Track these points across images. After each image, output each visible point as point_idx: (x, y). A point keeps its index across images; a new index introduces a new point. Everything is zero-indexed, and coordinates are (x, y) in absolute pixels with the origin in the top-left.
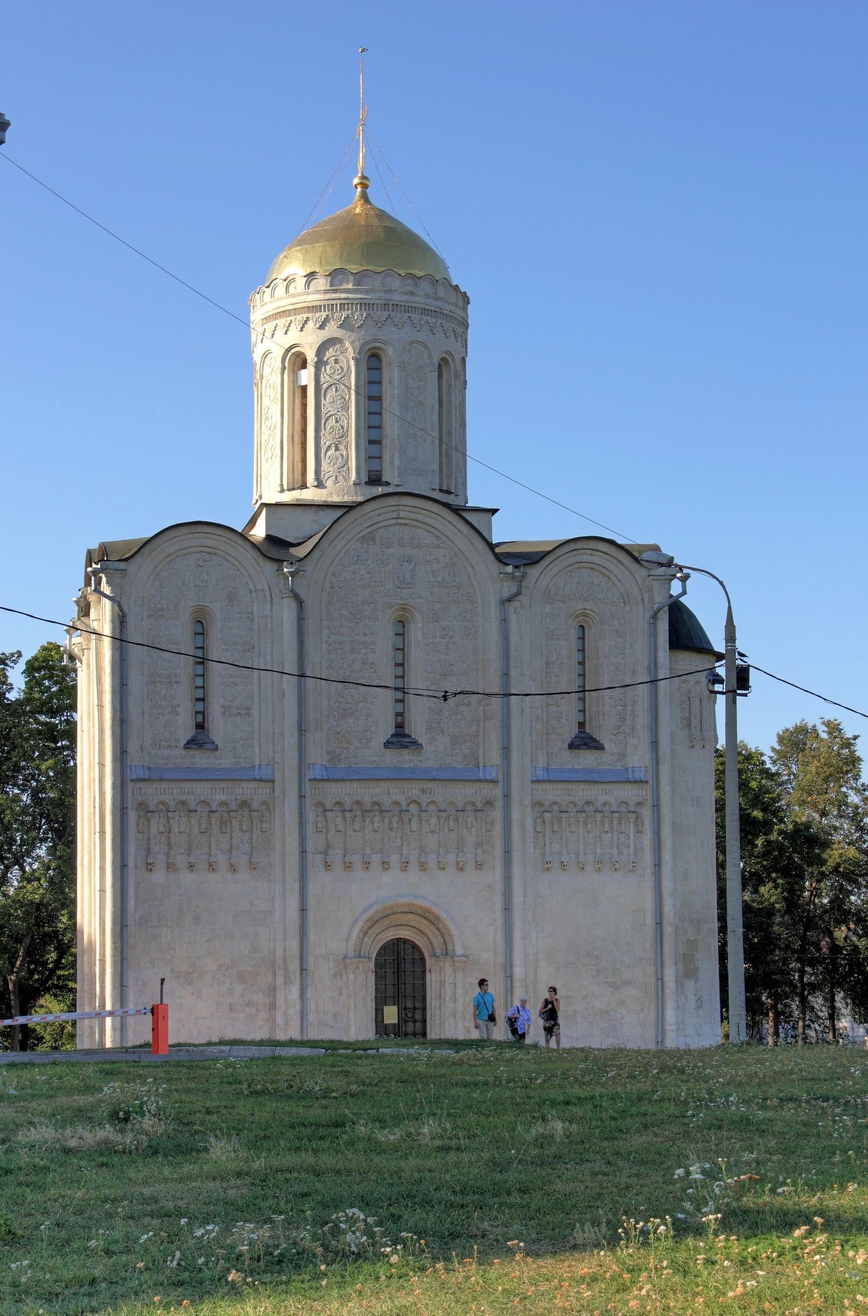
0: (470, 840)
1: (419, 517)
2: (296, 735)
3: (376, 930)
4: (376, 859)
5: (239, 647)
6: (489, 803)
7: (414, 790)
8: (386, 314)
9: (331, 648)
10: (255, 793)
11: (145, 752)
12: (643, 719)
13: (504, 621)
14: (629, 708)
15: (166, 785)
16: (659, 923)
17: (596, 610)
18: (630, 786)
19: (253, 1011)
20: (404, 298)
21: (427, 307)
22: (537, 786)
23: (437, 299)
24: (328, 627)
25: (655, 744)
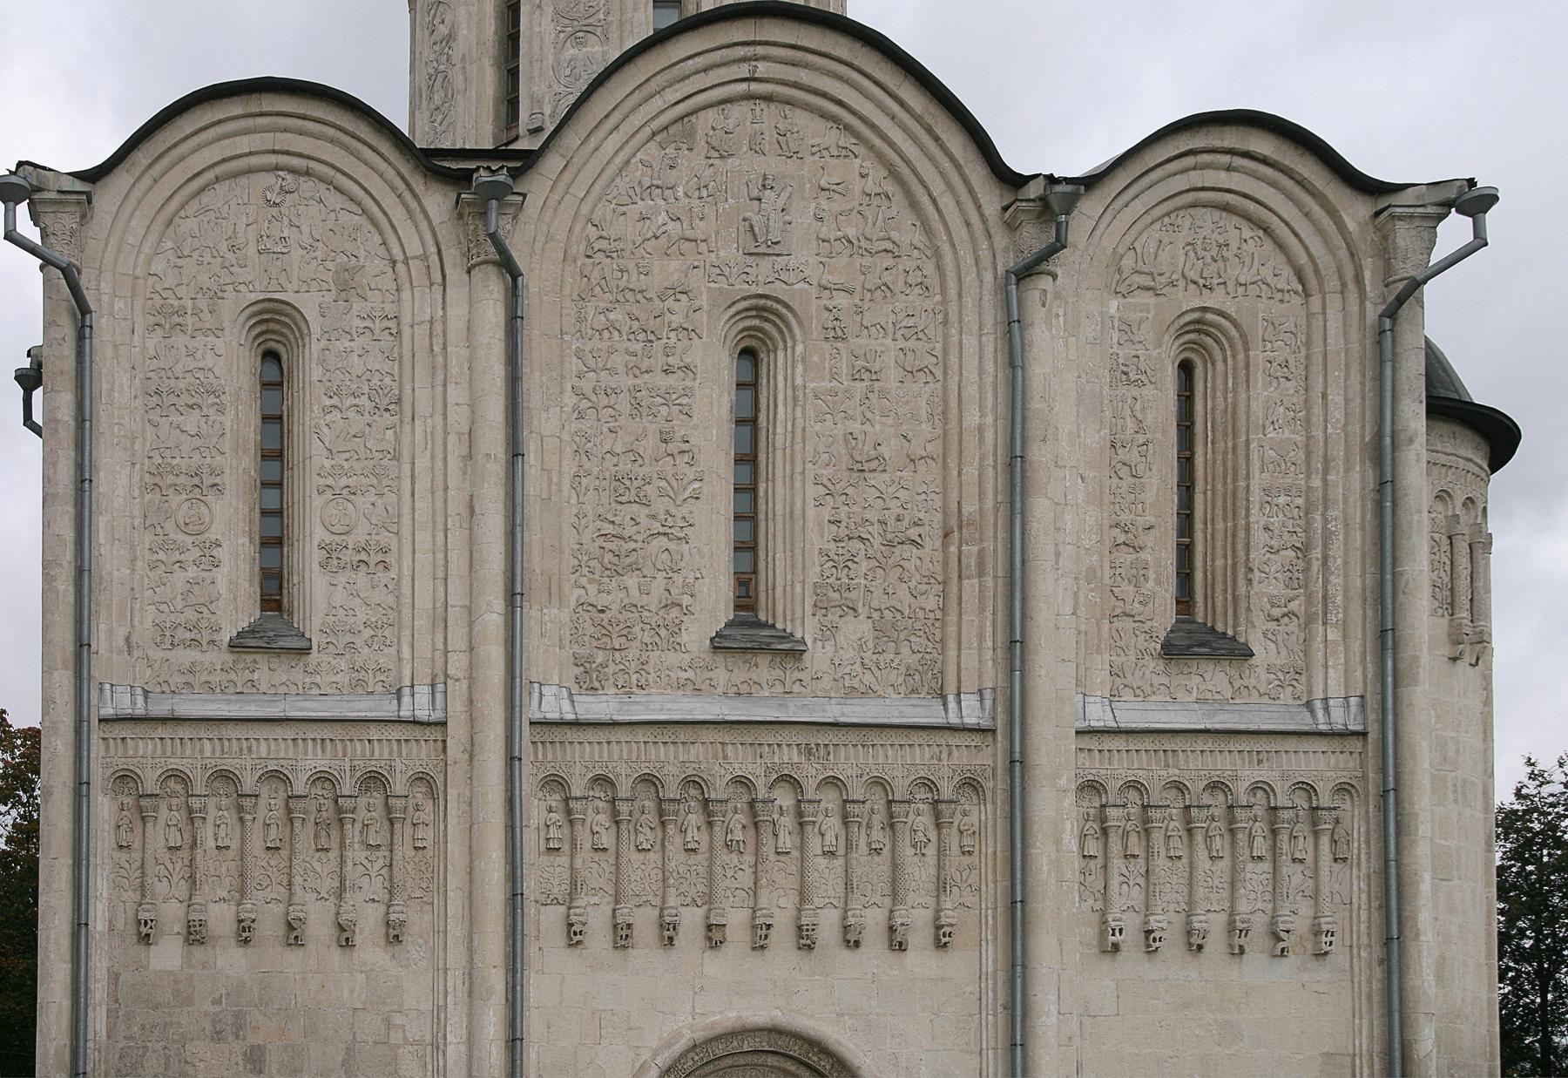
0: (919, 872)
1: (804, 76)
4: (691, 919)
5: (364, 400)
9: (585, 404)
11: (136, 653)
12: (1348, 576)
15: (185, 732)
17: (1232, 311)
18: (1319, 745)
22: (1087, 742)
24: (579, 354)
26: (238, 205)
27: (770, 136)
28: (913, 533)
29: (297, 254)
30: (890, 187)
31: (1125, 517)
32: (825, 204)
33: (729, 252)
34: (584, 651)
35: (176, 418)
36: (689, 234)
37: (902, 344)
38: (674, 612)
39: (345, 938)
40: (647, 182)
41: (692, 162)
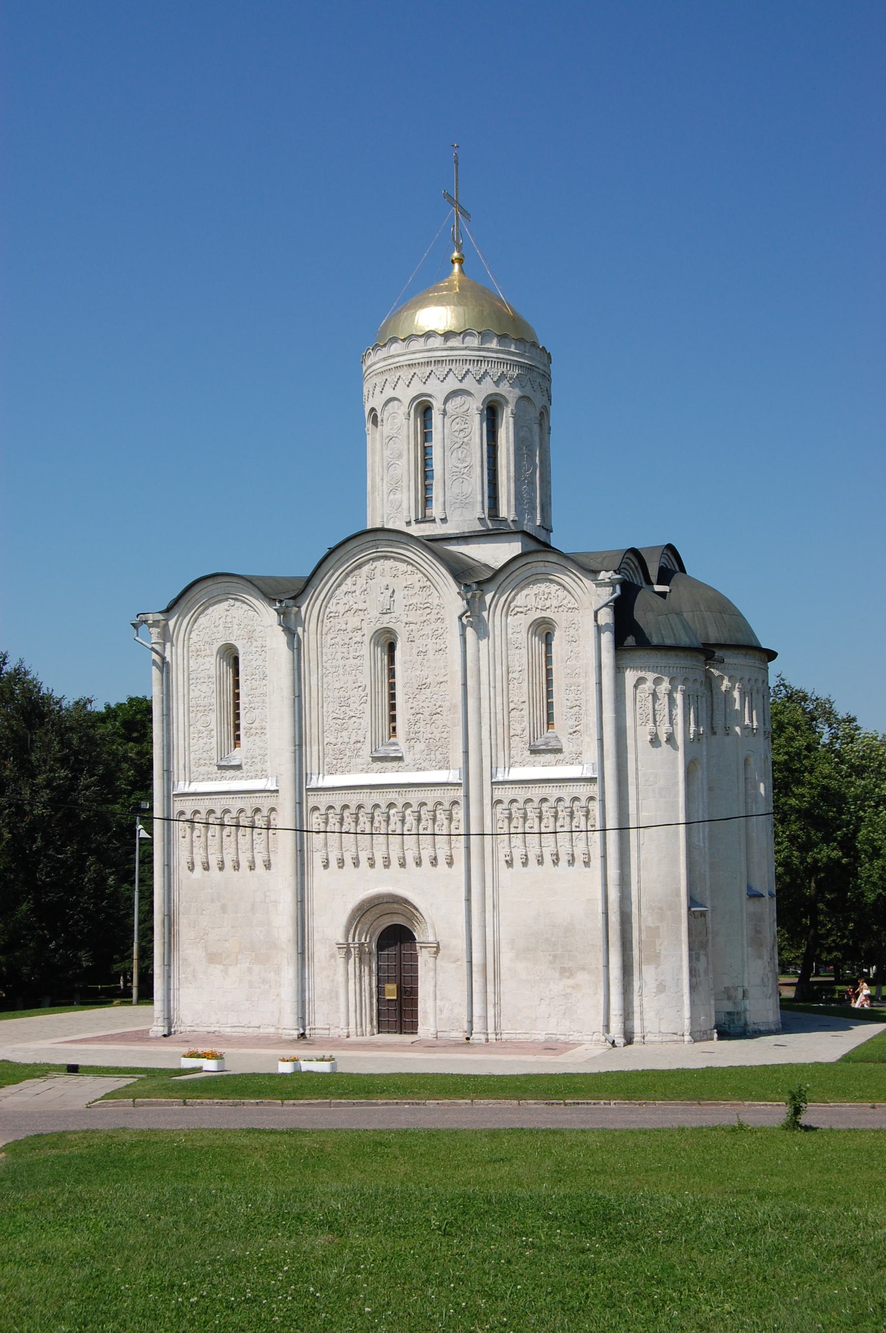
2: (291, 748)
3: (369, 917)
6: (455, 803)
7: (392, 796)
8: (429, 369)
10: (265, 803)
13: (463, 636)
14: (584, 708)
16: (606, 913)
19: (267, 987)
20: (445, 353)
21: (468, 358)
23: (479, 350)
25: (601, 740)
26: (218, 611)
27: (387, 569)
28: (438, 710)
29: (235, 627)
30: (429, 583)
31: (516, 699)
32: (406, 592)
33: (374, 613)
34: (330, 760)
35: (199, 687)
36: (360, 608)
37: (434, 641)
38: (359, 745)
39: (252, 868)
40: (345, 590)
41: (361, 581)
